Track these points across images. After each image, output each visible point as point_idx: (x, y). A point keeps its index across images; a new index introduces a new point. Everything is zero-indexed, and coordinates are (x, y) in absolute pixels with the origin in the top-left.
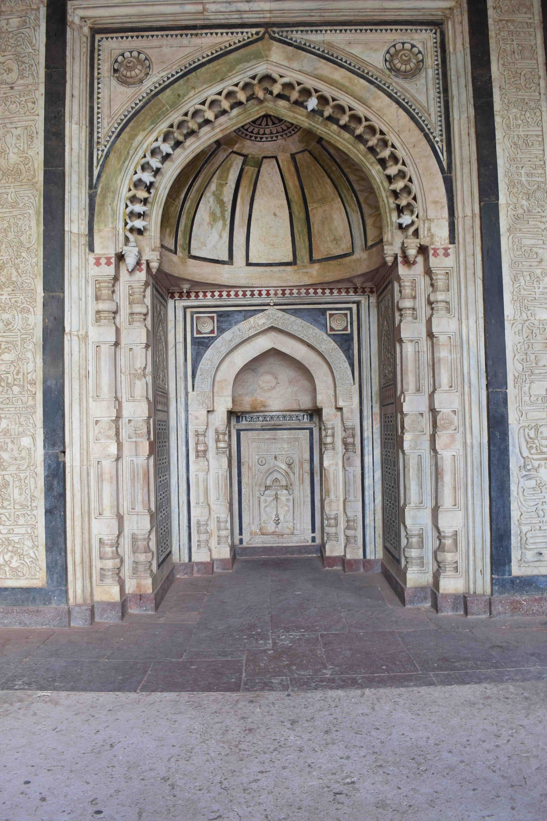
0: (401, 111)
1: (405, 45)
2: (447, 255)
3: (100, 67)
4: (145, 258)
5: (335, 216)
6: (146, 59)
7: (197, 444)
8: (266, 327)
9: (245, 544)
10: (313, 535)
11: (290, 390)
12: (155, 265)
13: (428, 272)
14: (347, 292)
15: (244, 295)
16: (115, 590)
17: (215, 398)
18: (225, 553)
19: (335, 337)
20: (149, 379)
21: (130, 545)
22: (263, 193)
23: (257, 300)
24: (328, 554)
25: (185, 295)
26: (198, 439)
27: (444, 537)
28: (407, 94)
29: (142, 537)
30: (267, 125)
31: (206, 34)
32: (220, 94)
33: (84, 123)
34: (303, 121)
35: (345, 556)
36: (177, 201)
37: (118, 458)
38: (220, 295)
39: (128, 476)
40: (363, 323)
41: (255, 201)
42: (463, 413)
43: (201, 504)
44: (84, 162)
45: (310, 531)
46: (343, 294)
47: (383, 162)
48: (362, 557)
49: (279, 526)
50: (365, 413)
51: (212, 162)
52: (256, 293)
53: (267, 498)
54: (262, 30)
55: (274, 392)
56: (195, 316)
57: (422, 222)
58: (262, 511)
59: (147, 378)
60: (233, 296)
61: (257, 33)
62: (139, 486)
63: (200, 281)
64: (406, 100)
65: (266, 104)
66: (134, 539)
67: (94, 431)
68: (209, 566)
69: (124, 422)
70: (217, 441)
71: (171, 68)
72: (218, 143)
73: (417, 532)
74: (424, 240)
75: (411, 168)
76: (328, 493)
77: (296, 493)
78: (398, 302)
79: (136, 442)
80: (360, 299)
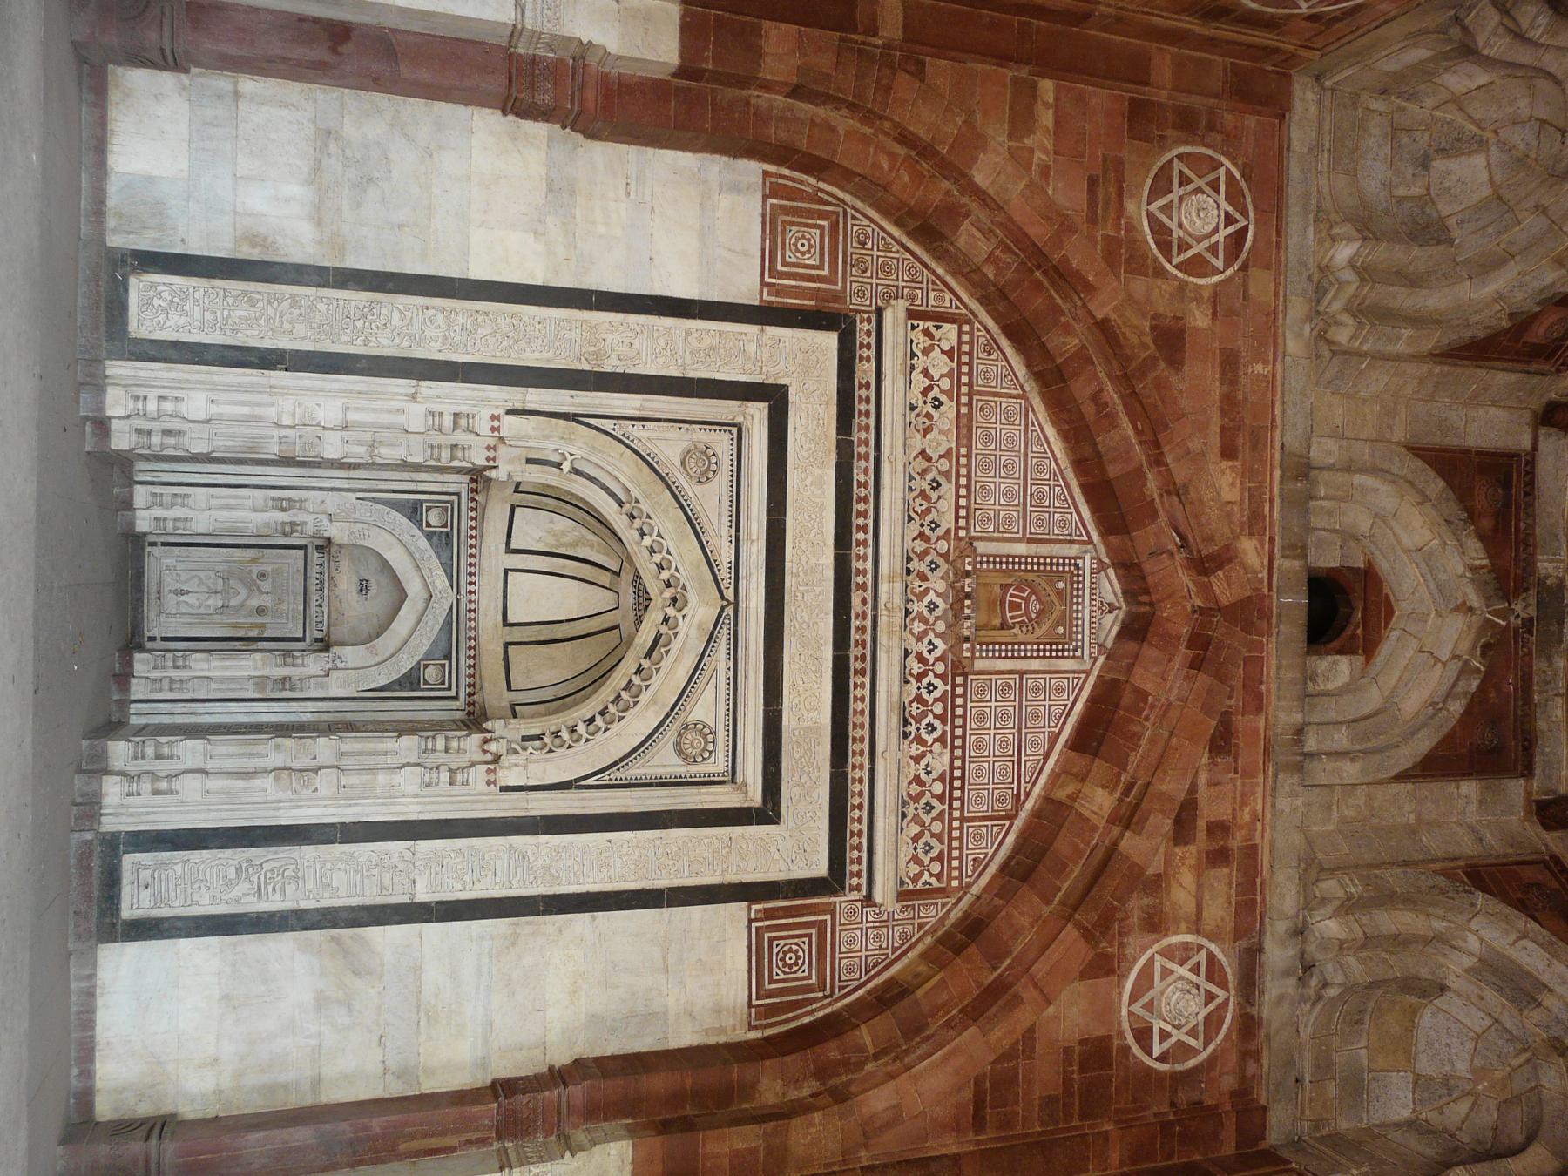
2: (489, 783)
7: (290, 500)
12: (493, 474)
14: (469, 685)
19: (416, 668)
24: (137, 656)
27: (170, 782)
32: (669, 553)
37: (278, 425)
47: (592, 720)
52: (473, 579)
54: (732, 599)
66: (180, 433)
68: (128, 505)
77: (218, 618)
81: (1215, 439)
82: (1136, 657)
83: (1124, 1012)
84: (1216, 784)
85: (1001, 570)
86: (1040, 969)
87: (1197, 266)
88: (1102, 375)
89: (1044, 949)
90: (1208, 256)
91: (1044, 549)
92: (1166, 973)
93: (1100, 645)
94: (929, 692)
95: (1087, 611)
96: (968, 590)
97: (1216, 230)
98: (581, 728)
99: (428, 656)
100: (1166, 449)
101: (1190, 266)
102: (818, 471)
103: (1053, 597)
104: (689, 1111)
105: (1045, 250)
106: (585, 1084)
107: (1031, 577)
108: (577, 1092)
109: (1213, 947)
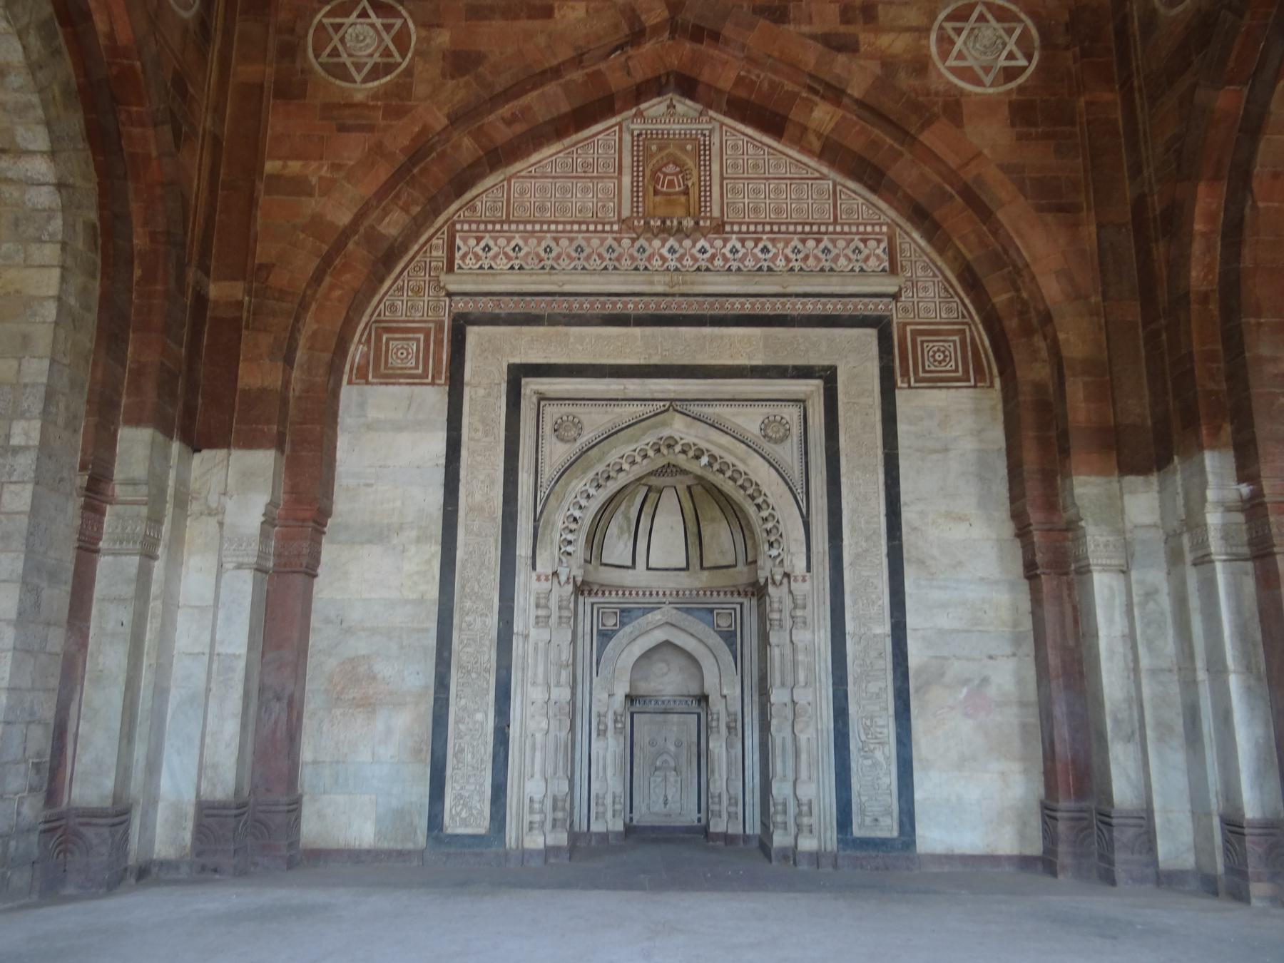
0: (772, 470)
2: (804, 580)
7: (599, 724)
12: (579, 580)
19: (720, 633)
23: (654, 599)
47: (758, 506)
54: (668, 404)
66: (555, 800)
68: (604, 837)
70: (616, 721)
76: (713, 771)
77: (684, 774)
81: (538, 24)
82: (709, 86)
83: (991, 91)
84: (811, 18)
85: (644, 196)
86: (953, 161)
87: (401, 40)
88: (492, 117)
89: (938, 159)
90: (393, 32)
91: (627, 161)
92: (960, 56)
93: (701, 114)
94: (737, 251)
95: (675, 126)
96: (659, 223)
97: (373, 26)
98: (765, 514)
100: (547, 65)
101: (403, 48)
102: (572, 340)
103: (664, 153)
104: (1053, 433)
105: (397, 166)
106: (1029, 510)
107: (648, 173)
108: (1035, 517)
109: (941, 16)
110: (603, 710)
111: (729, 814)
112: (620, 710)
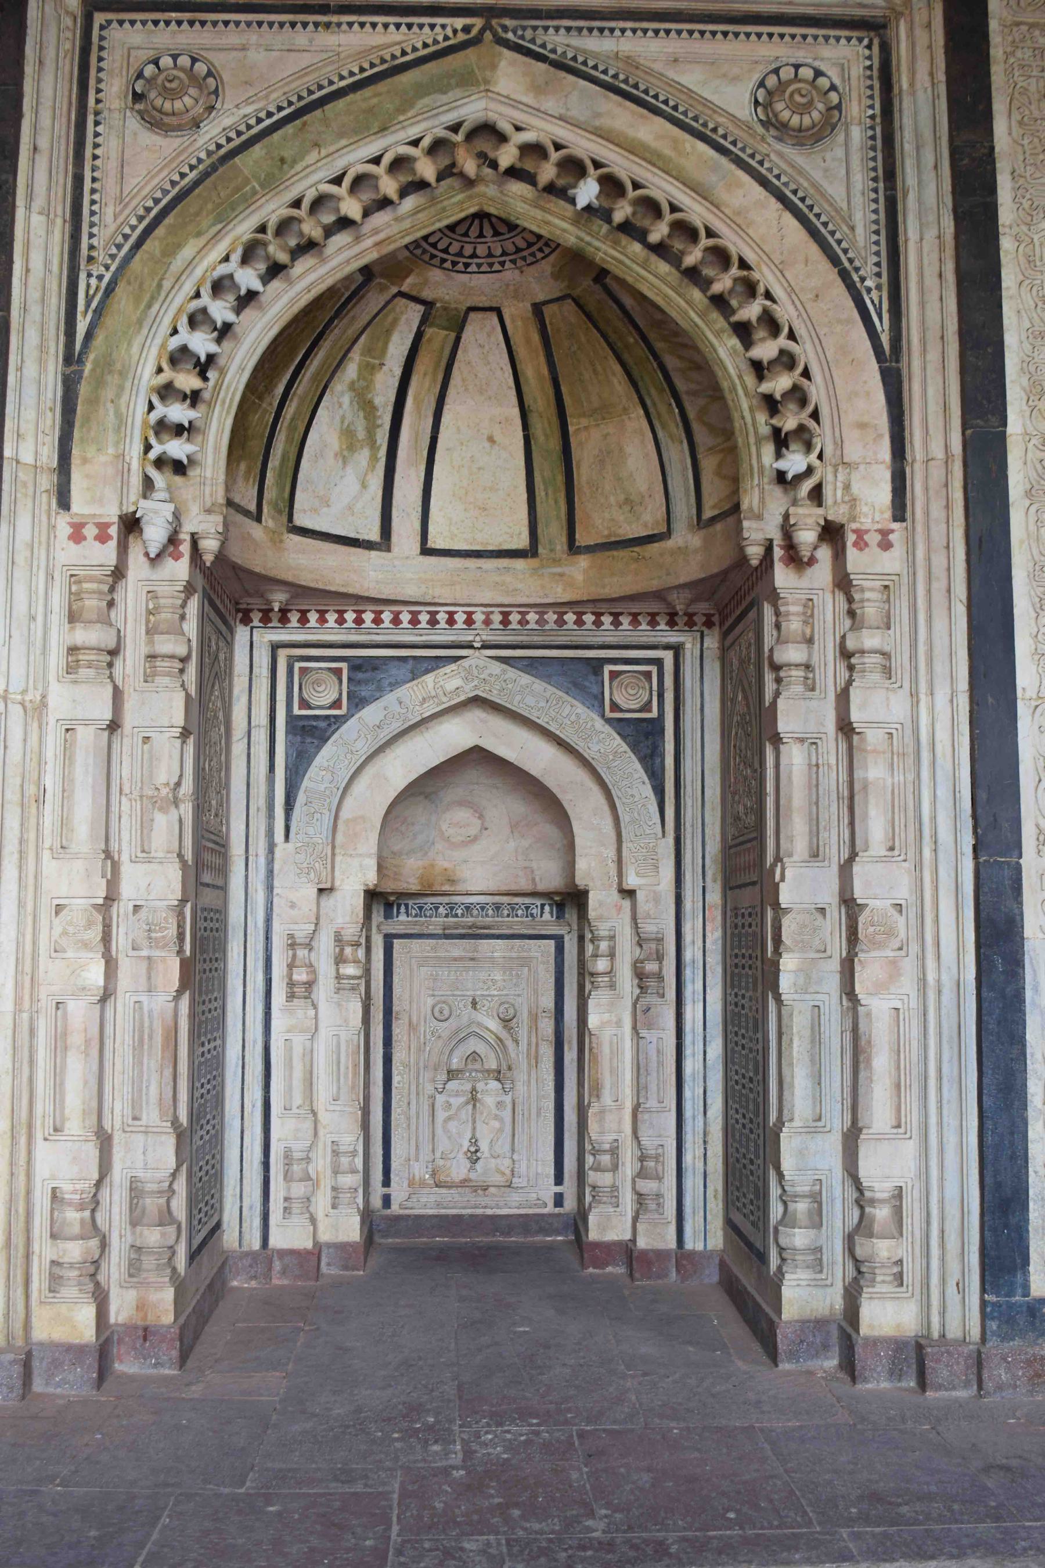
1: (801, 70)
2: (886, 545)
3: (102, 86)
4: (189, 527)
5: (629, 449)
6: (210, 74)
7: (291, 966)
8: (462, 698)
9: (395, 1208)
10: (558, 1189)
11: (512, 844)
12: (210, 545)
13: (843, 583)
14: (653, 623)
15: (414, 621)
16: (86, 1315)
17: (338, 859)
18: (348, 1228)
19: (621, 726)
20: (187, 810)
21: (125, 1207)
22: (466, 390)
25: (275, 616)
26: (294, 956)
27: (872, 1202)
28: (801, 181)
29: (154, 1187)
30: (481, 235)
31: (350, 25)
32: (376, 161)
33: (60, 212)
34: (564, 230)
35: (634, 1241)
36: (268, 400)
37: (107, 995)
38: (359, 621)
39: (128, 1040)
40: (688, 695)
41: (446, 408)
42: (919, 910)
43: (295, 1110)
44: (56, 303)
45: (552, 1180)
46: (644, 627)
47: (743, 331)
48: (673, 1245)
49: (479, 1166)
50: (688, 905)
51: (351, 314)
52: (442, 617)
53: (452, 1100)
54: (478, 22)
55: (476, 847)
56: (297, 665)
57: (830, 469)
58: (439, 1131)
59: (182, 806)
60: (387, 624)
61: (466, 29)
62: (153, 1062)
63: (312, 585)
64: (800, 194)
65: (481, 188)
66: (136, 1191)
67: (50, 929)
68: (307, 1260)
69: (122, 911)
70: (340, 960)
71: (267, 96)
72: (367, 272)
73: (807, 1188)
74: (836, 513)
75: (809, 346)
76: (597, 1090)
77: (521, 1088)
78: (771, 650)
79: (149, 958)
80: (681, 639)
99: (596, 701)
110: (303, 930)
111: (640, 1198)
112: (352, 930)
